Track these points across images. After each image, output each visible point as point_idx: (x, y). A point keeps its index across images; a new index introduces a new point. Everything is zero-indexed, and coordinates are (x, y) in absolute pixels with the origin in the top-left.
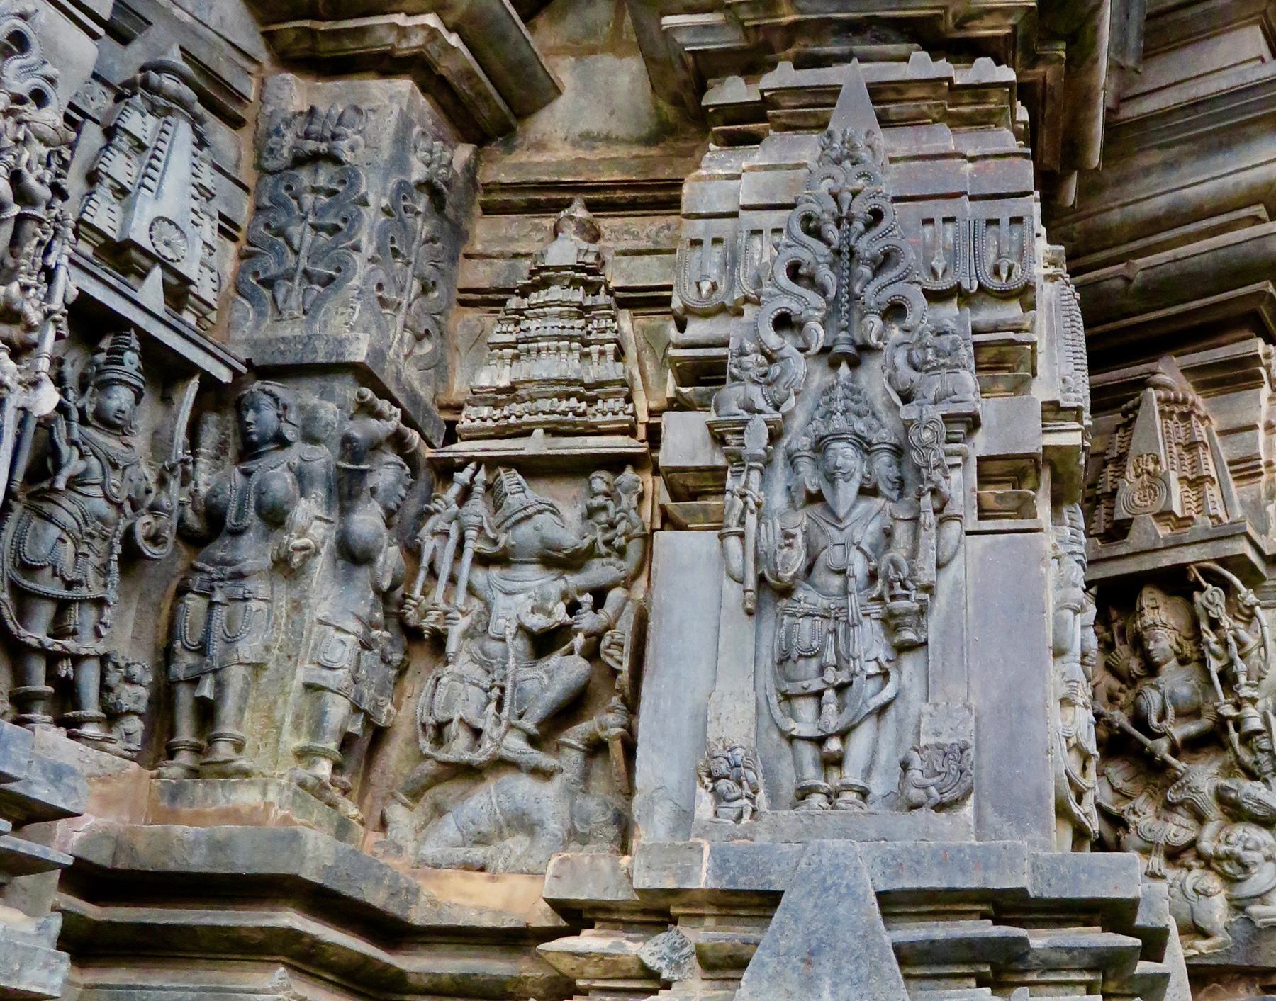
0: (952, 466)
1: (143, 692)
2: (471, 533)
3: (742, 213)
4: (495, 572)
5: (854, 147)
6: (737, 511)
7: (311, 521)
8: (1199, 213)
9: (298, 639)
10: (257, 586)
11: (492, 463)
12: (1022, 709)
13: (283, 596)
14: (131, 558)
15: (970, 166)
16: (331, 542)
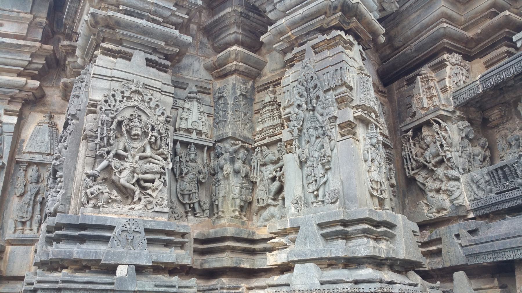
0: (332, 129)
1: (208, 205)
2: (259, 161)
3: (291, 84)
4: (264, 167)
5: (307, 64)
6: (294, 149)
7: (228, 168)
8: (428, 26)
9: (231, 189)
10: (222, 182)
11: (261, 146)
12: (351, 178)
13: (226, 182)
14: (200, 183)
15: (331, 58)
16: (232, 171)
